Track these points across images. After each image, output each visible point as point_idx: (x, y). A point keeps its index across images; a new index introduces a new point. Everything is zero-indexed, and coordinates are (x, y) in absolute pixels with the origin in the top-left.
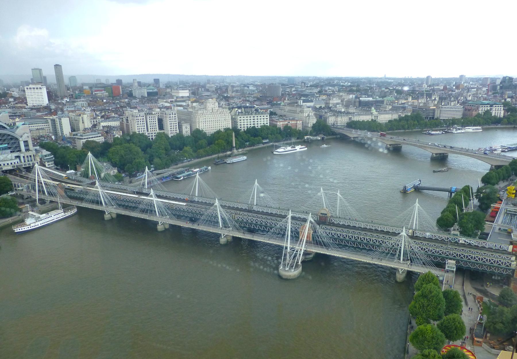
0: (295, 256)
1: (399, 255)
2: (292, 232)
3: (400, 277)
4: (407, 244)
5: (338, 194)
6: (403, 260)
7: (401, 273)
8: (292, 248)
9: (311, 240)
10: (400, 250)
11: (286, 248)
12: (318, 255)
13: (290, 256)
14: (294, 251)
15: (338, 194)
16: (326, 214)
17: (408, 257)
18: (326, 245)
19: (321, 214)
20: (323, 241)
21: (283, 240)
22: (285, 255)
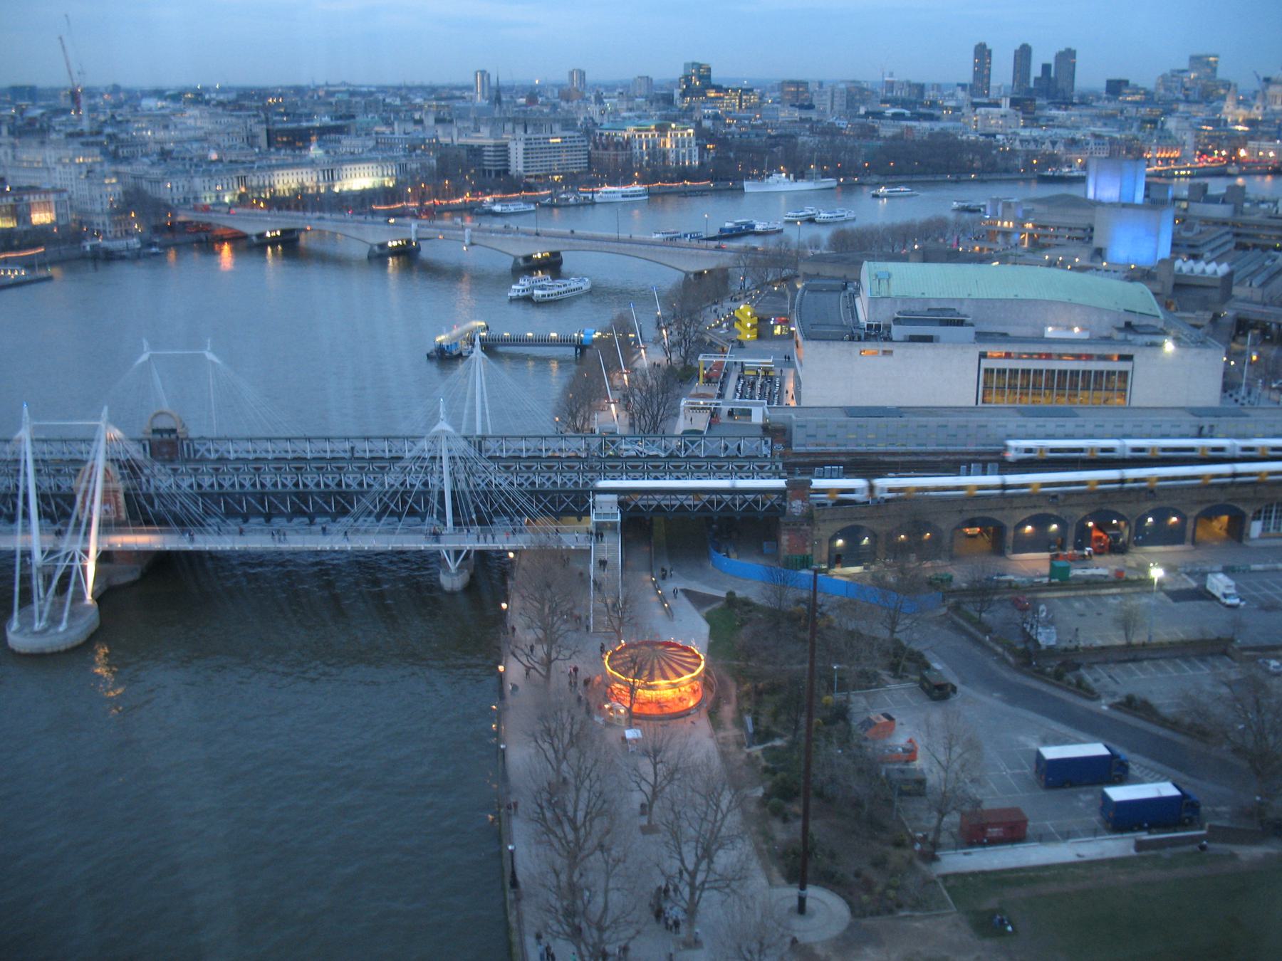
0: (66, 577)
1: (442, 515)
2: (42, 497)
3: (452, 579)
4: (462, 477)
5: (210, 356)
6: (456, 524)
7: (453, 566)
8: (51, 553)
9: (123, 515)
10: (442, 493)
11: (27, 554)
12: (160, 562)
13: (48, 579)
14: (57, 559)
15: (210, 356)
16: (174, 431)
17: (470, 515)
18: (182, 523)
19: (155, 431)
20: (170, 512)
21: (13, 532)
22: (26, 579)
